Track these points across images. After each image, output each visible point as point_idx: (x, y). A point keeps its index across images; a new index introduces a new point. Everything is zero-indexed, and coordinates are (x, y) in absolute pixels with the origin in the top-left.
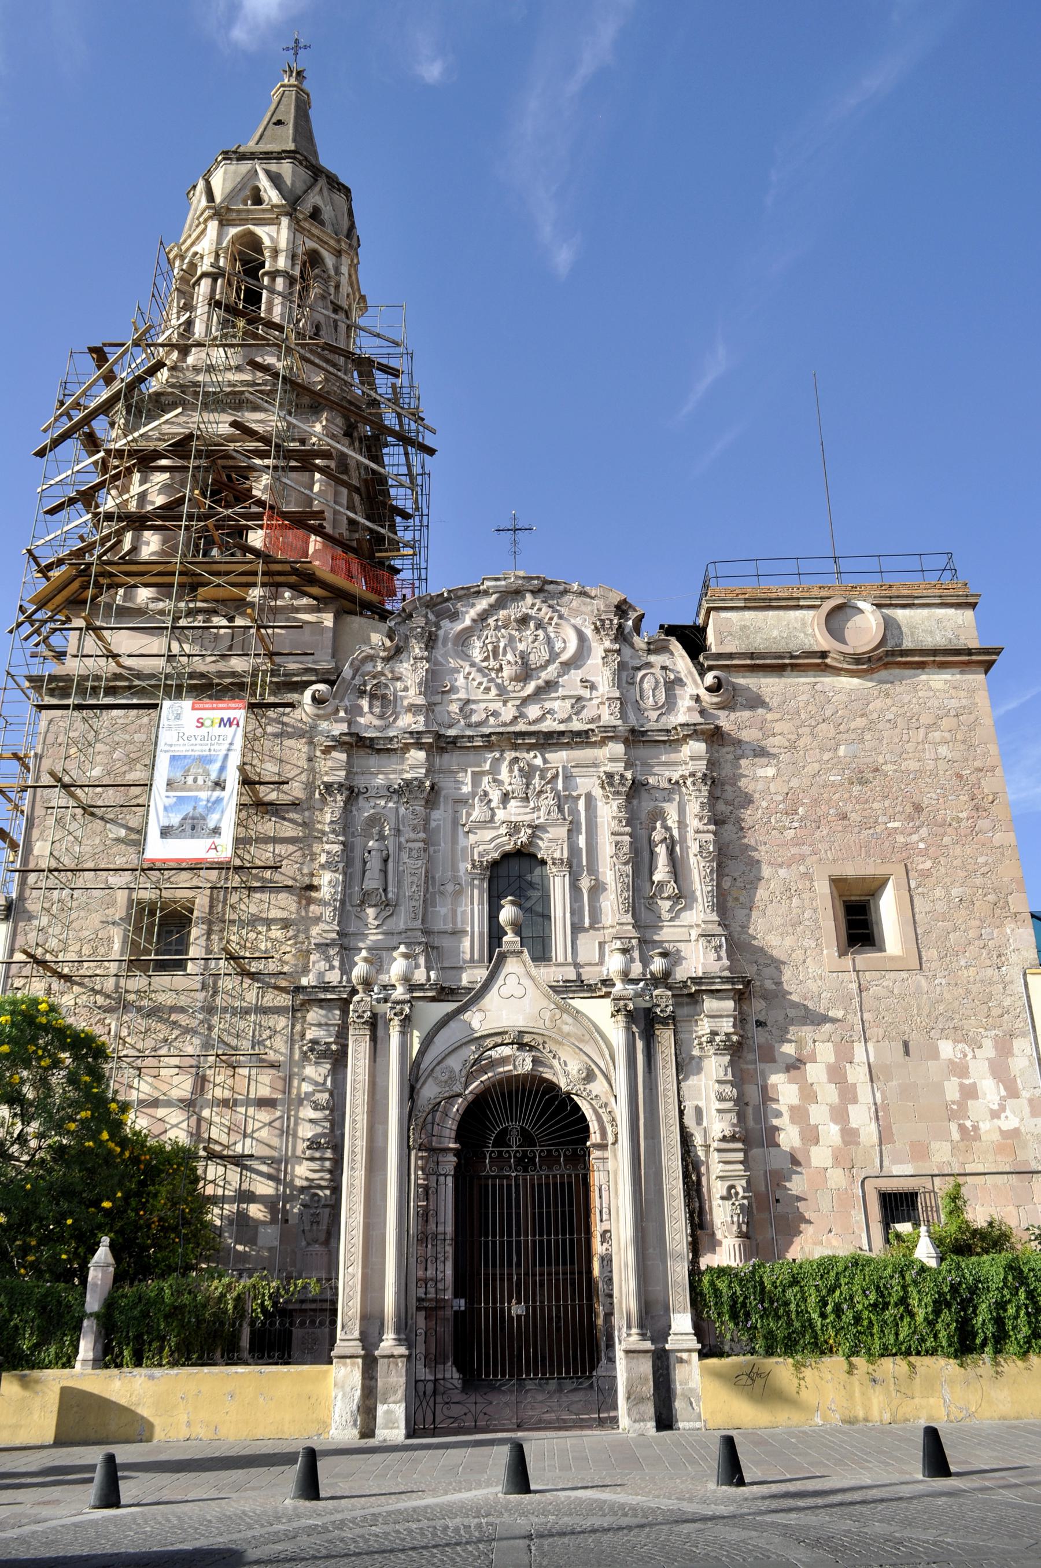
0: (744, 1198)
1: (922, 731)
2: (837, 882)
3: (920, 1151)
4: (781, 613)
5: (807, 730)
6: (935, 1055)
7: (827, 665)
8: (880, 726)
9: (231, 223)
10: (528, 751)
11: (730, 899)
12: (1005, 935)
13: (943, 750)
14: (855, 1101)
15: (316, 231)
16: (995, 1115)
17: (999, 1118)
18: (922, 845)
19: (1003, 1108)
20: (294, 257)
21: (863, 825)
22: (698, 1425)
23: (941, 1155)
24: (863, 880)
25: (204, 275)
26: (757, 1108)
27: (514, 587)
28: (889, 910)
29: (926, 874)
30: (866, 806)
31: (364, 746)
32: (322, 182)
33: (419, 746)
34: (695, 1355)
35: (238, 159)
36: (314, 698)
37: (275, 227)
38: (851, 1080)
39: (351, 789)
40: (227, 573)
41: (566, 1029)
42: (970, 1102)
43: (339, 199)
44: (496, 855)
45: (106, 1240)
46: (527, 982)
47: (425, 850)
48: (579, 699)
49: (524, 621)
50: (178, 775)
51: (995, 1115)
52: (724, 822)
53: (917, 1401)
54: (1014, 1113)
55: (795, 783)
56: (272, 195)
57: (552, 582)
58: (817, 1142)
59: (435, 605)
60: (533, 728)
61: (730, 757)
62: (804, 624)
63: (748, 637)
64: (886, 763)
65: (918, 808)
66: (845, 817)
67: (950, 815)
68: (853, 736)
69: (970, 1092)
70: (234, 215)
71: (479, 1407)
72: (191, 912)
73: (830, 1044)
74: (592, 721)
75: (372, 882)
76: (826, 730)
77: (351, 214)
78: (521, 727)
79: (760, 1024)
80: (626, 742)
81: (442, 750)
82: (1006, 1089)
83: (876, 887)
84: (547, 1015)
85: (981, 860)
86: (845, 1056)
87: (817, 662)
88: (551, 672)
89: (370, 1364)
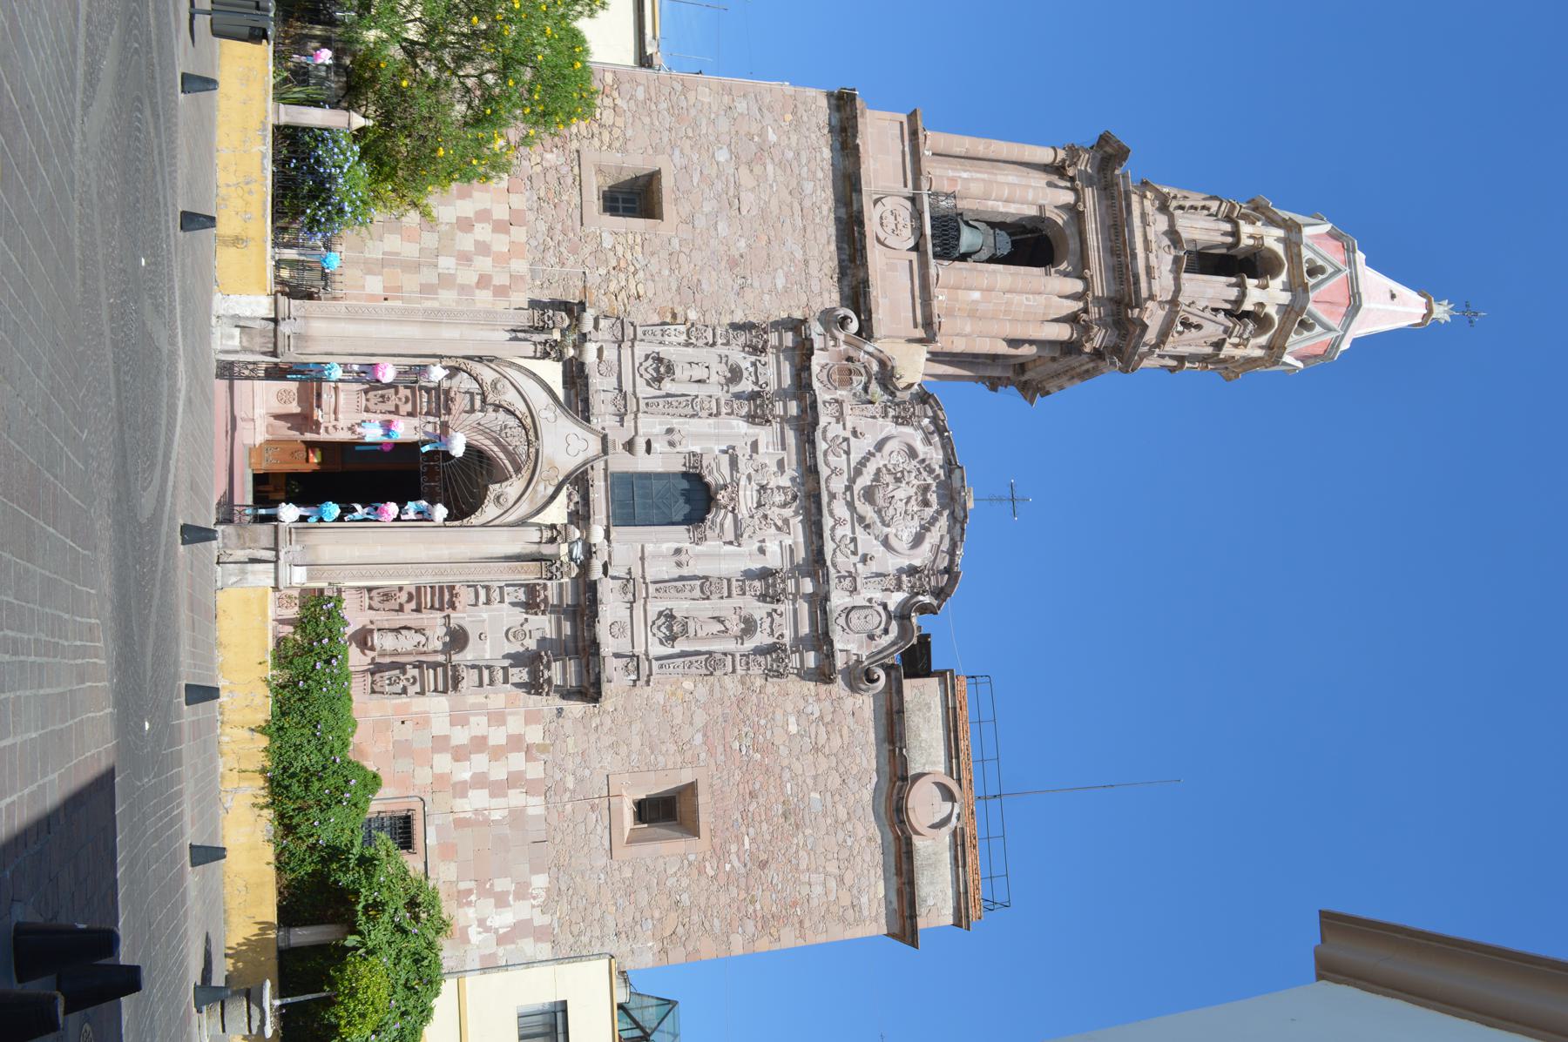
2: (692, 788)
3: (448, 851)
6: (535, 870)
8: (841, 835)
13: (818, 890)
14: (493, 795)
16: (481, 922)
18: (728, 867)
19: (488, 930)
24: (695, 811)
25: (1236, 225)
33: (803, 410)
36: (845, 318)
38: (511, 792)
41: (541, 488)
44: (709, 479)
51: (481, 922)
55: (784, 751)
62: (934, 763)
65: (763, 865)
66: (753, 795)
68: (829, 805)
69: (501, 901)
73: (542, 775)
78: (825, 498)
79: (560, 711)
85: (716, 922)
86: (531, 788)
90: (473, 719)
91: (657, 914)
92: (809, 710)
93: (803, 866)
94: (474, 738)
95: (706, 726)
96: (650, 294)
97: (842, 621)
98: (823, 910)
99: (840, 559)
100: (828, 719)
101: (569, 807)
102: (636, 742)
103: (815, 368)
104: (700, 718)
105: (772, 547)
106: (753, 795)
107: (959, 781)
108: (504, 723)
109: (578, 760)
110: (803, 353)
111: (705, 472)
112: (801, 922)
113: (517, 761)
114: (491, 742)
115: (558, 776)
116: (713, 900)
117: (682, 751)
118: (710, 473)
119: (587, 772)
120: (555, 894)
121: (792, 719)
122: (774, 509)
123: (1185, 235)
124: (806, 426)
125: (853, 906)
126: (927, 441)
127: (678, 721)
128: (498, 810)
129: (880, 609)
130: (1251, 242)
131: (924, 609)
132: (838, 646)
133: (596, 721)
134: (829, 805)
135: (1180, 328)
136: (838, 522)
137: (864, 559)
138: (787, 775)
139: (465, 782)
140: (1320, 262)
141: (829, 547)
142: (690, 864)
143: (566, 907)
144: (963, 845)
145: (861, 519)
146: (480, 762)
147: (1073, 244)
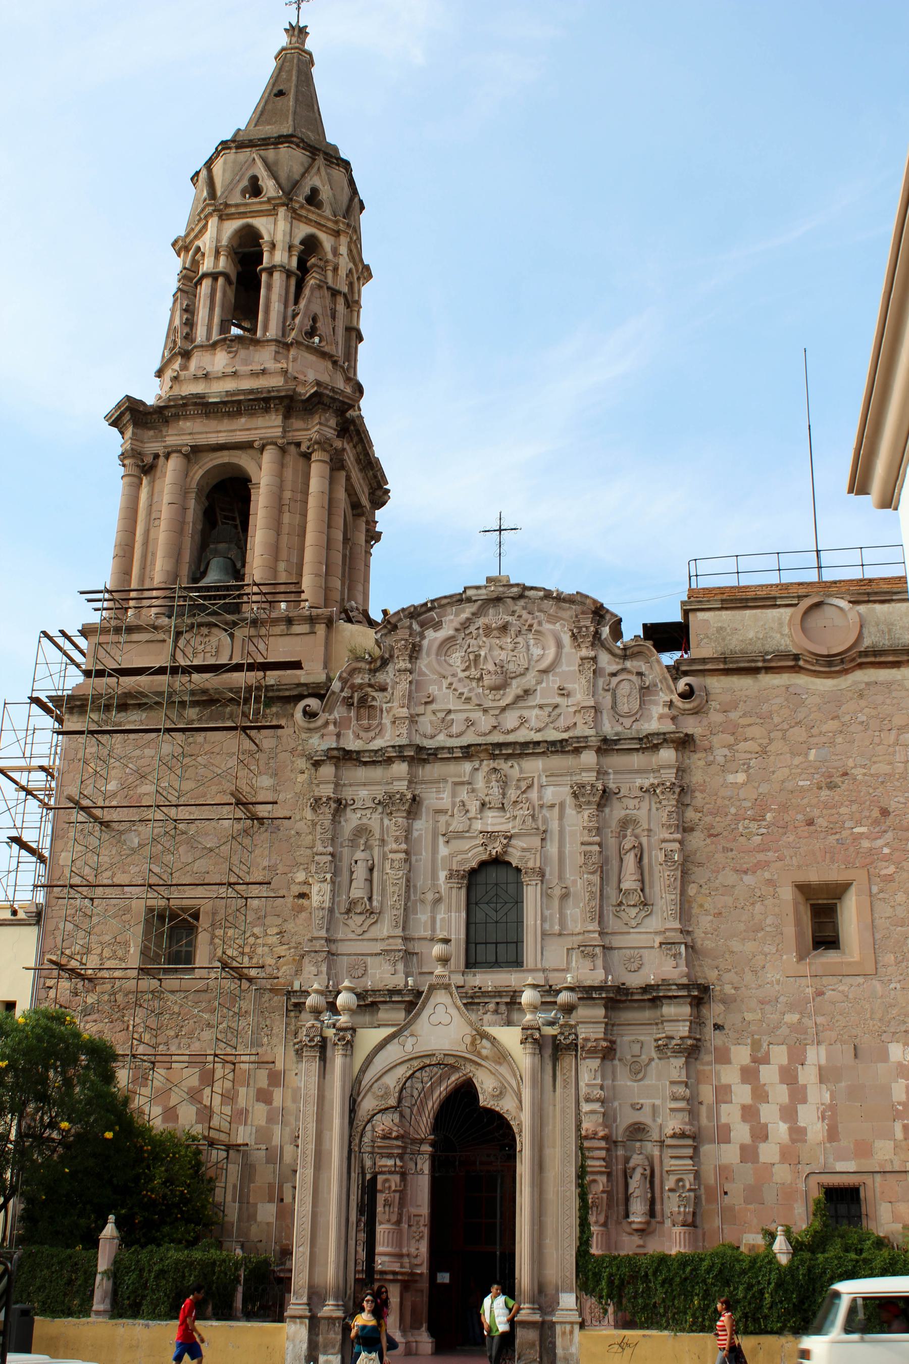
0: (690, 1190)
1: (894, 732)
2: (804, 889)
3: (863, 1149)
5: (780, 734)
7: (801, 668)
9: (230, 217)
11: (695, 905)
14: (804, 1101)
15: (312, 217)
18: (886, 850)
20: (290, 248)
21: (831, 830)
25: (205, 275)
26: (710, 1109)
27: (494, 595)
28: (851, 917)
29: (889, 879)
30: (834, 811)
31: (351, 759)
32: (320, 161)
33: (403, 758)
34: (577, 1327)
35: (237, 148)
37: (271, 219)
38: (801, 1081)
39: (339, 801)
43: (338, 174)
44: (474, 864)
45: (112, 1218)
47: (406, 861)
48: (556, 707)
49: (504, 628)
52: (692, 830)
55: (764, 788)
56: (269, 187)
57: (532, 588)
58: (766, 1138)
59: (420, 615)
60: (511, 738)
61: (701, 763)
62: (781, 624)
63: (724, 639)
64: (855, 767)
65: (885, 812)
66: (810, 823)
68: (823, 739)
70: (233, 210)
73: (784, 1047)
74: (567, 729)
75: (358, 891)
76: (798, 734)
77: (352, 182)
79: (717, 1027)
80: (599, 751)
81: (425, 761)
83: (839, 890)
86: (797, 1058)
87: (792, 663)
88: (529, 680)
89: (314, 1323)
90: (724, 1120)
92: (721, 760)
93: (886, 769)
96: (280, 921)
97: (627, 722)
99: (562, 723)
100: (731, 739)
101: (820, 1020)
105: (550, 794)
107: (800, 597)
108: (727, 1089)
109: (768, 1008)
110: (344, 757)
111: (467, 867)
113: (769, 1074)
114: (748, 1100)
121: (731, 778)
123: (215, 337)
124: (421, 756)
126: (437, 626)
128: (818, 1095)
129: (615, 680)
130: (222, 260)
131: (617, 633)
133: (729, 990)
135: (317, 339)
136: (523, 721)
137: (563, 692)
138: (789, 785)
140: (245, 183)
142: (881, 891)
144: (868, 594)
145: (518, 698)
146: (769, 1113)
147: (224, 457)
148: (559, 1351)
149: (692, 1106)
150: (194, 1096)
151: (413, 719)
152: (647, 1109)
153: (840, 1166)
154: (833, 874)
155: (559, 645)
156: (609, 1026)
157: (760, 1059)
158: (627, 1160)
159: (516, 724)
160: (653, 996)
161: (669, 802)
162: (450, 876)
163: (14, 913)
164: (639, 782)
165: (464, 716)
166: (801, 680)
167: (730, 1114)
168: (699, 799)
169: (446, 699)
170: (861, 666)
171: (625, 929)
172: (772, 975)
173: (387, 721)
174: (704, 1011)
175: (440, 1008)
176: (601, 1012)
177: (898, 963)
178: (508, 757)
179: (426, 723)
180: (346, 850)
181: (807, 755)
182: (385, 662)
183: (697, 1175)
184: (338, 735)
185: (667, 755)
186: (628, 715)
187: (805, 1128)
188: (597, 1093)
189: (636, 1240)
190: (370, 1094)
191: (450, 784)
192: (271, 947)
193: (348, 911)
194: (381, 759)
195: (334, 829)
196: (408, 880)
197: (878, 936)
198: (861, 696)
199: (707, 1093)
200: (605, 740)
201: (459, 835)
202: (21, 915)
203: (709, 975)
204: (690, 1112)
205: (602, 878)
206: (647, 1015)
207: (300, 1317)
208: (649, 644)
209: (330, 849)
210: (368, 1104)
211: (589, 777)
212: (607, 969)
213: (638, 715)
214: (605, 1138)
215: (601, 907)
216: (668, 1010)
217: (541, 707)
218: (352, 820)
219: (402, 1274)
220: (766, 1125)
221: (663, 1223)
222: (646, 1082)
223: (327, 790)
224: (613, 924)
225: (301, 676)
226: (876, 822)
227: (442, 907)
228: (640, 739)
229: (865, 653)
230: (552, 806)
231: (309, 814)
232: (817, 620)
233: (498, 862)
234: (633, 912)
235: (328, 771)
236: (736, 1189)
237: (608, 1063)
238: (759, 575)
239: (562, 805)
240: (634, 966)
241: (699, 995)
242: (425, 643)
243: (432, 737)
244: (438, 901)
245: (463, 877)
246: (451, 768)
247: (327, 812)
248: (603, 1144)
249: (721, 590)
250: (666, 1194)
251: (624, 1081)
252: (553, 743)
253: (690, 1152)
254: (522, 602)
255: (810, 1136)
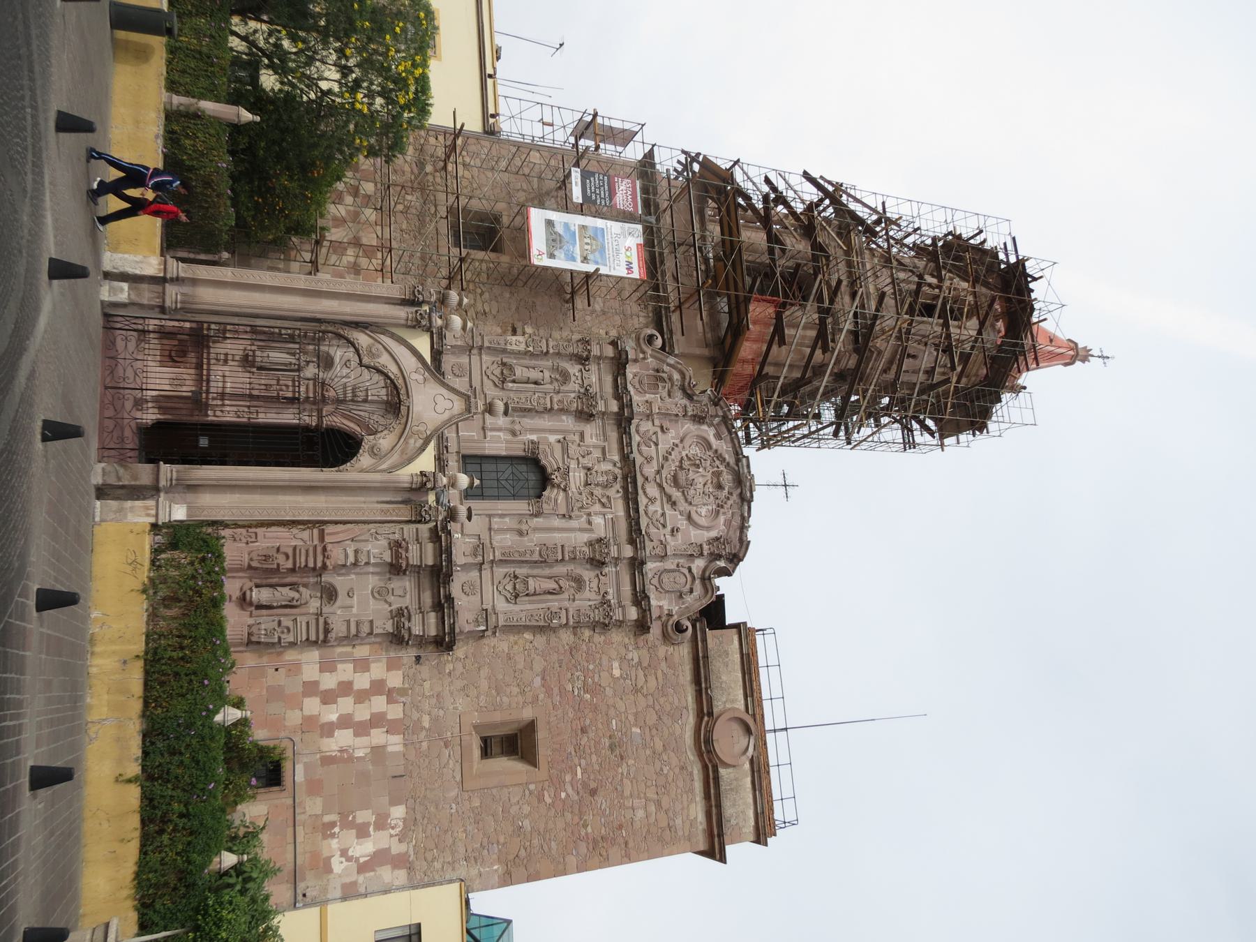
0: (280, 638)
2: (531, 727)
3: (314, 787)
4: (741, 683)
6: (394, 802)
10: (623, 487)
11: (516, 637)
12: (492, 864)
13: (640, 814)
14: (356, 735)
16: (344, 853)
17: (342, 856)
18: (563, 795)
19: (349, 859)
21: (578, 748)
22: (97, 519)
23: (312, 806)
29: (540, 799)
31: (619, 369)
33: (621, 408)
34: (152, 520)
38: (374, 732)
39: (587, 359)
40: (734, 270)
41: (412, 441)
42: (354, 831)
44: (544, 462)
45: (258, 119)
46: (446, 416)
47: (546, 409)
48: (664, 526)
49: (720, 487)
50: (590, 233)
51: (344, 853)
52: (575, 634)
53: (106, 697)
54: (346, 869)
55: (609, 692)
58: (324, 702)
59: (726, 423)
60: (640, 491)
62: (733, 701)
65: (593, 792)
66: (584, 730)
67: (589, 817)
68: (648, 739)
69: (362, 832)
71: (126, 416)
72: (493, 250)
73: (401, 716)
76: (652, 718)
79: (418, 658)
81: (619, 425)
82: (365, 862)
84: (422, 428)
87: (705, 712)
88: (682, 505)
89: (160, 281)
90: (340, 666)
91: (502, 840)
92: (630, 656)
93: (627, 793)
94: (340, 684)
95: (544, 671)
96: (494, 312)
97: (655, 581)
98: (645, 830)
99: (653, 530)
100: (645, 664)
101: (425, 744)
102: (484, 684)
103: (629, 376)
104: (539, 665)
105: (598, 521)
106: (584, 730)
107: (754, 716)
108: (367, 669)
110: (620, 364)
111: (541, 457)
112: (626, 843)
113: (379, 703)
114: (356, 687)
115: (415, 716)
116: (551, 825)
117: (523, 692)
118: (546, 456)
119: (441, 713)
120: (410, 823)
121: (616, 664)
122: (599, 488)
124: (623, 421)
125: (670, 827)
126: (718, 436)
127: (521, 666)
128: (361, 747)
129: (686, 571)
132: (653, 602)
133: (449, 667)
134: (648, 739)
136: (652, 500)
137: (674, 531)
138: (612, 712)
139: (332, 723)
141: (644, 522)
143: (421, 835)
144: (759, 771)
145: (669, 498)
146: (346, 705)
148: (129, 504)
149: (351, 639)
150: (356, 243)
151: (649, 416)
152: (348, 602)
153: (299, 768)
154: (543, 752)
155: (708, 528)
156: (418, 569)
157: (391, 696)
158: (305, 586)
159: (650, 495)
160: (443, 605)
161: (598, 616)
162: (533, 442)
163: (493, 116)
164: (611, 591)
165: (654, 456)
166: (691, 720)
167: (345, 671)
168: (599, 639)
169: (666, 441)
170: (705, 767)
171: (496, 582)
172: (461, 703)
173: (648, 397)
174: (431, 648)
175: (449, 405)
176: (430, 562)
177: (472, 809)
178: (625, 489)
179: (646, 426)
180: (550, 363)
181: (636, 725)
182: (690, 397)
183: (293, 645)
184: (636, 361)
185: (633, 614)
186: (660, 581)
187: (332, 736)
188: (363, 559)
189: (236, 594)
190: (371, 341)
191: (602, 444)
192: (474, 305)
193: (504, 364)
194: (620, 393)
195: (566, 355)
196: (530, 410)
197: (494, 791)
198: (682, 768)
199: (362, 651)
200: (643, 563)
201: (565, 450)
202: (491, 121)
203: (460, 651)
204: (347, 637)
205: (536, 562)
206: (427, 598)
207: (165, 269)
208: (714, 598)
209: (551, 351)
210: (362, 339)
211: (614, 551)
212: (466, 567)
213: (660, 588)
214: (324, 567)
215: (513, 562)
216: (432, 618)
217: (663, 514)
218: (573, 369)
219: (207, 398)
220: (335, 702)
221: (251, 616)
222: (372, 601)
223: (595, 351)
224: (500, 571)
225: (677, 336)
226: (585, 785)
227: (509, 437)
228: (644, 591)
229: (716, 771)
230: (590, 523)
231: (576, 337)
232: (737, 730)
233: (544, 480)
234: (509, 587)
235: (609, 351)
236: (280, 678)
237: (387, 569)
238: (768, 682)
239: (591, 530)
240: (466, 589)
241: (444, 642)
242: (705, 427)
243: (637, 431)
244: (514, 433)
245: (533, 453)
246: (615, 446)
247: (579, 349)
248: (319, 564)
249: (755, 653)
250: (277, 619)
251: (373, 581)
252: (638, 523)
253: (313, 638)
254: (738, 501)
255: (326, 740)
